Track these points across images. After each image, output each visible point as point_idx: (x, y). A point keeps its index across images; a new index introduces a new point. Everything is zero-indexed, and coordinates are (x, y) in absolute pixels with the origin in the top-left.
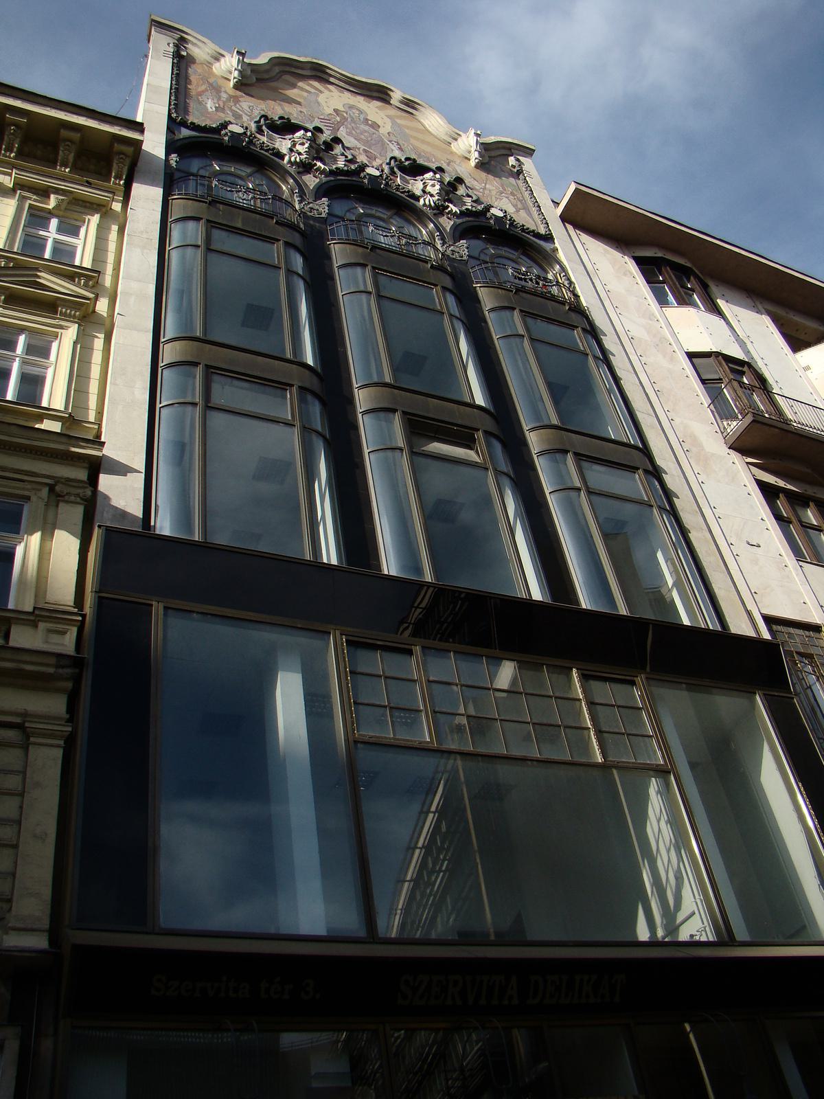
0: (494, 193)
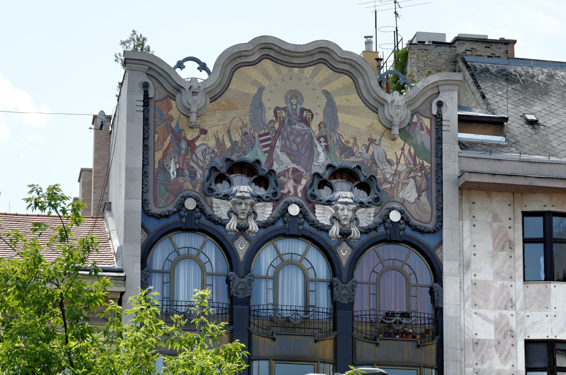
0: (403, 176)
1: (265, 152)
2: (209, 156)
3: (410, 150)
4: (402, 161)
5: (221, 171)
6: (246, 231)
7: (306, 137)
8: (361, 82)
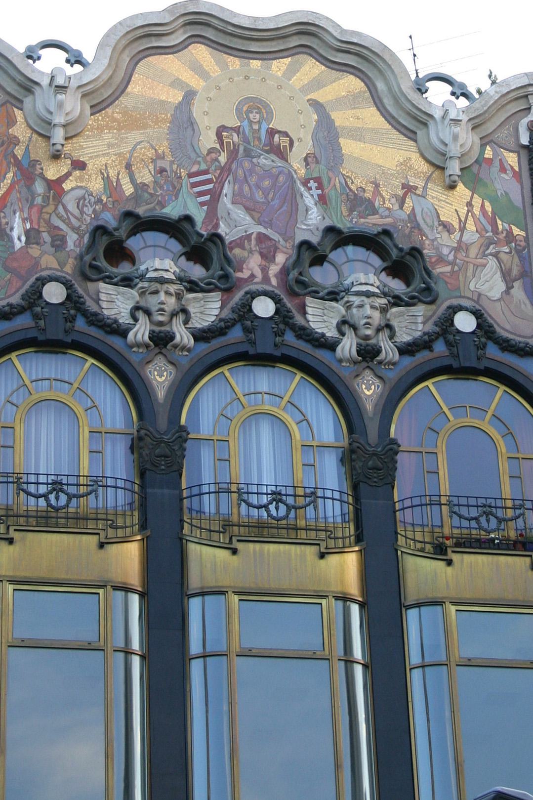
0: (473, 252)
1: (202, 204)
2: (91, 210)
3: (483, 206)
4: (471, 226)
5: (116, 234)
6: (169, 347)
7: (281, 179)
8: (380, 85)
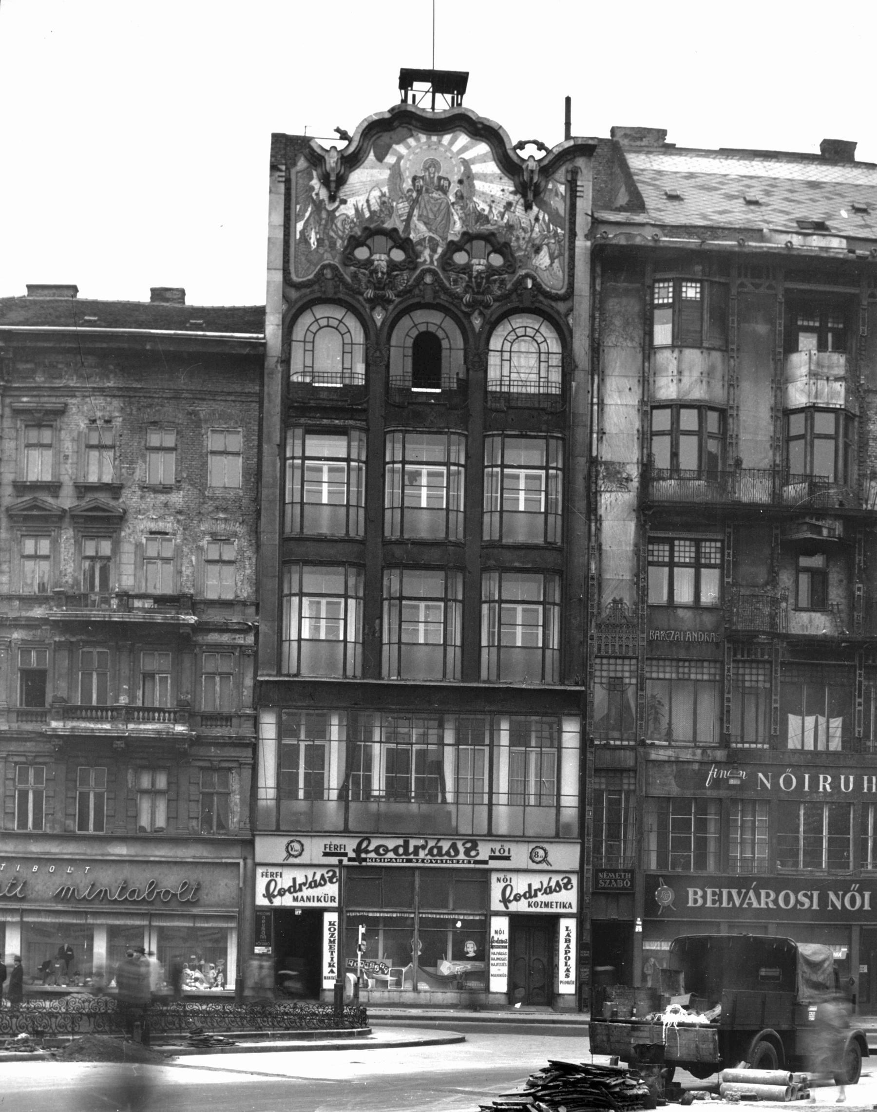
1: (403, 221)
3: (544, 217)
